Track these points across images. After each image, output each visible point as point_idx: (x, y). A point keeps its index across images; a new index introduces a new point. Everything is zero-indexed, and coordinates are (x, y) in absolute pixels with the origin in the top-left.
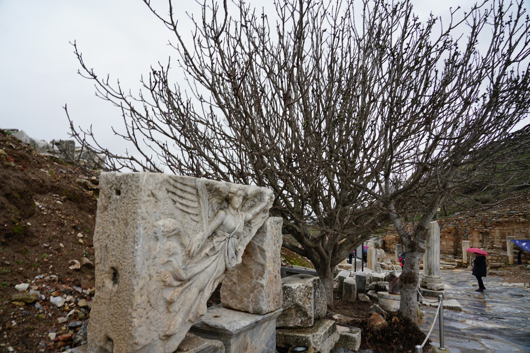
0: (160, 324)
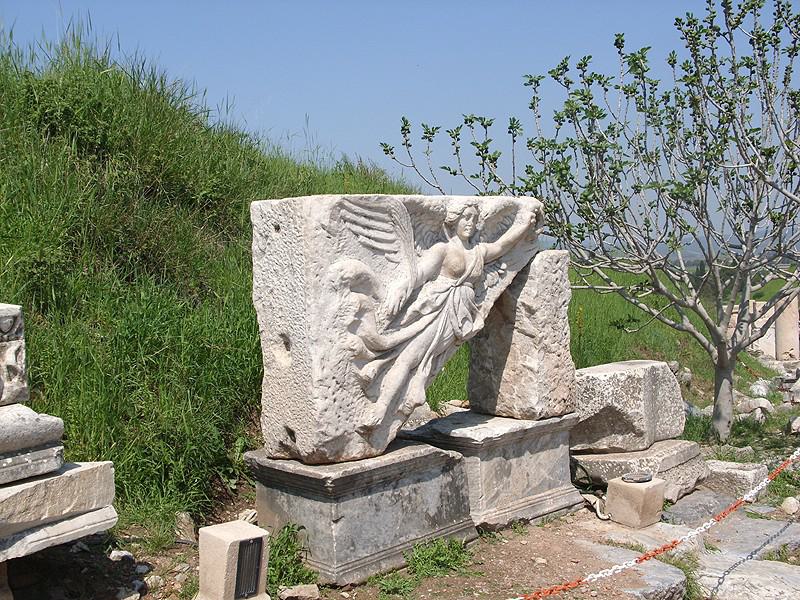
0: (354, 410)
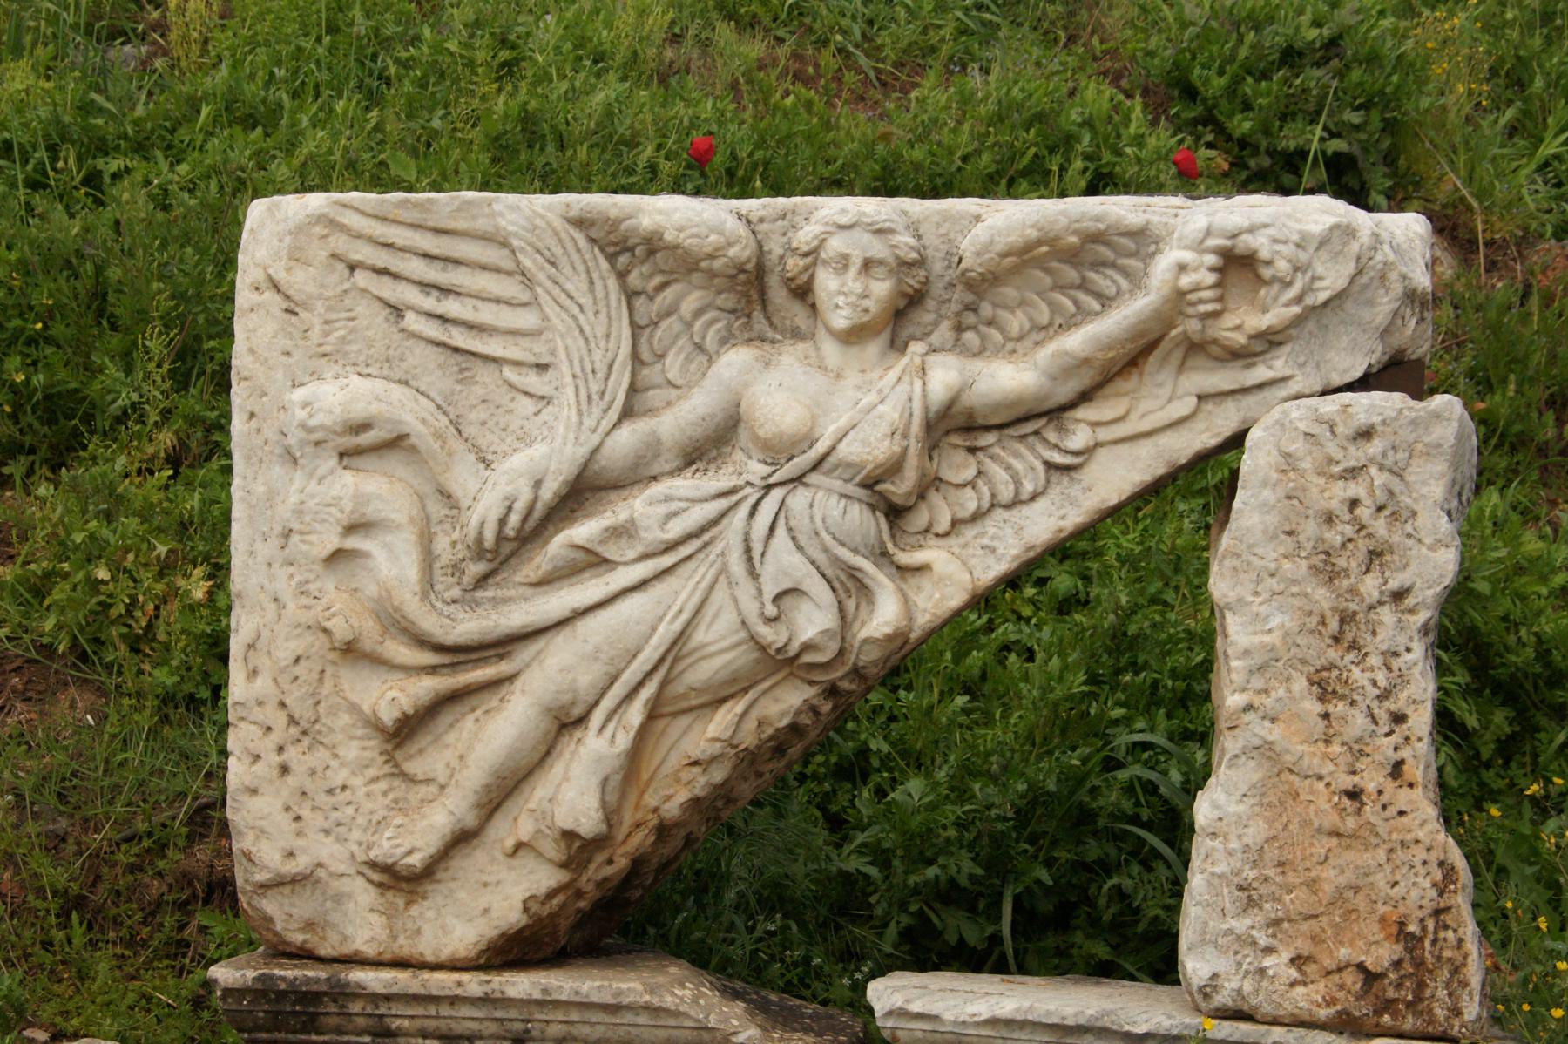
0: (350, 810)
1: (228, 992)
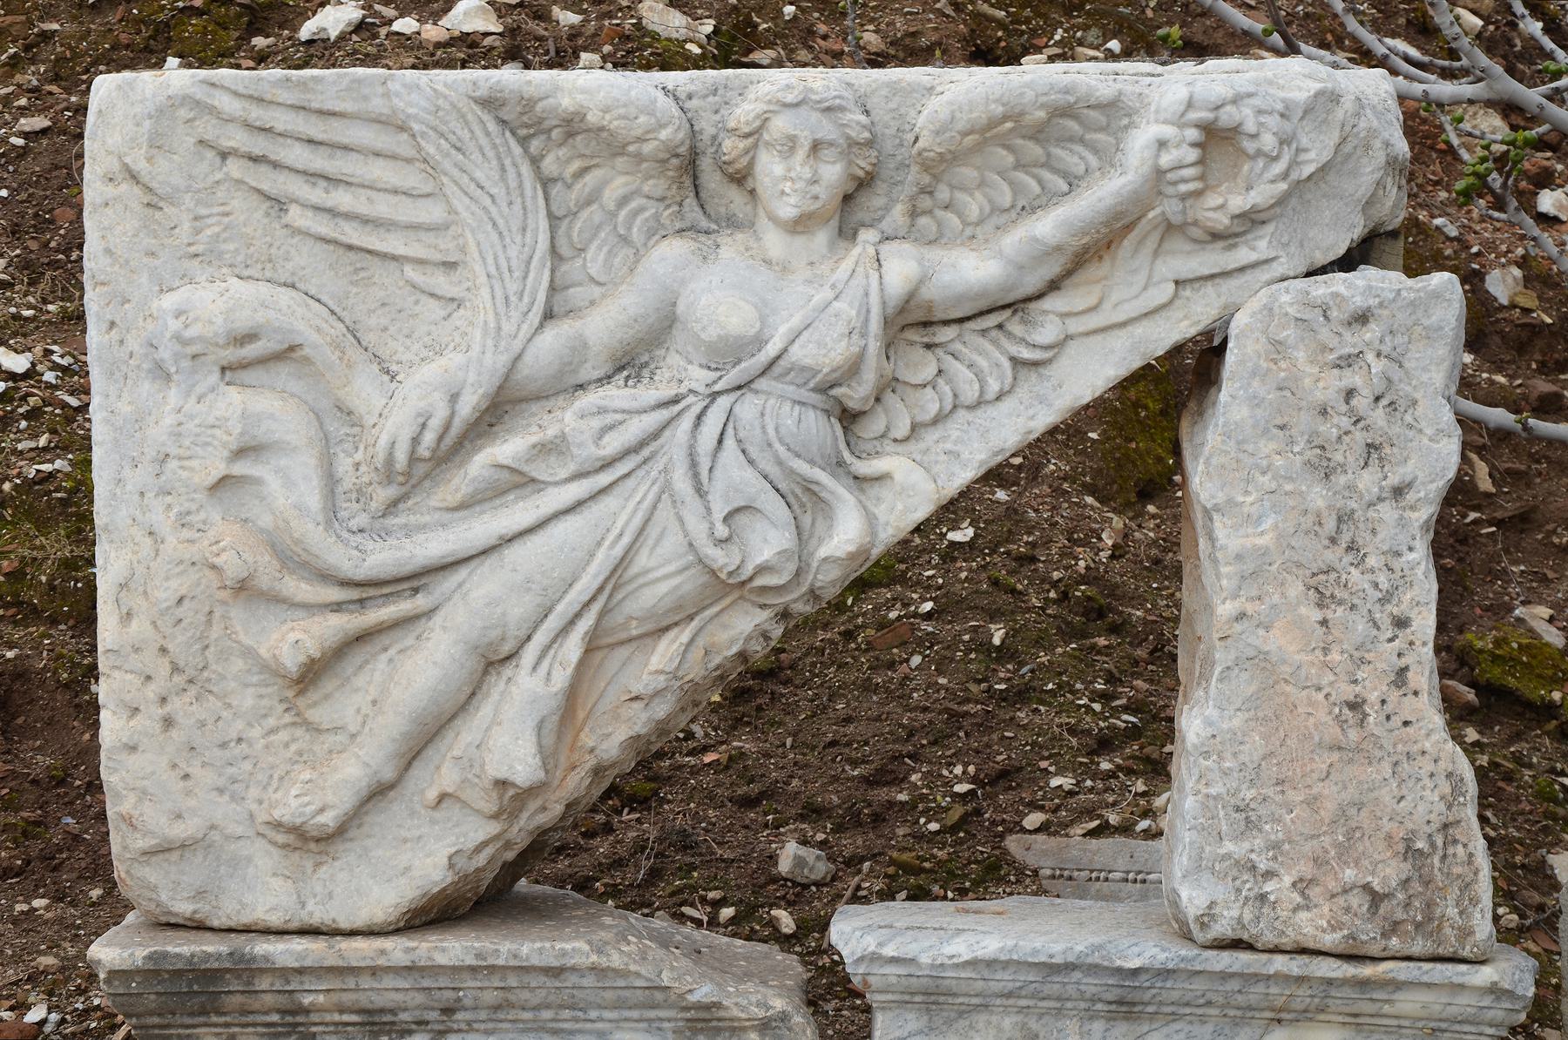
1: (114, 974)
